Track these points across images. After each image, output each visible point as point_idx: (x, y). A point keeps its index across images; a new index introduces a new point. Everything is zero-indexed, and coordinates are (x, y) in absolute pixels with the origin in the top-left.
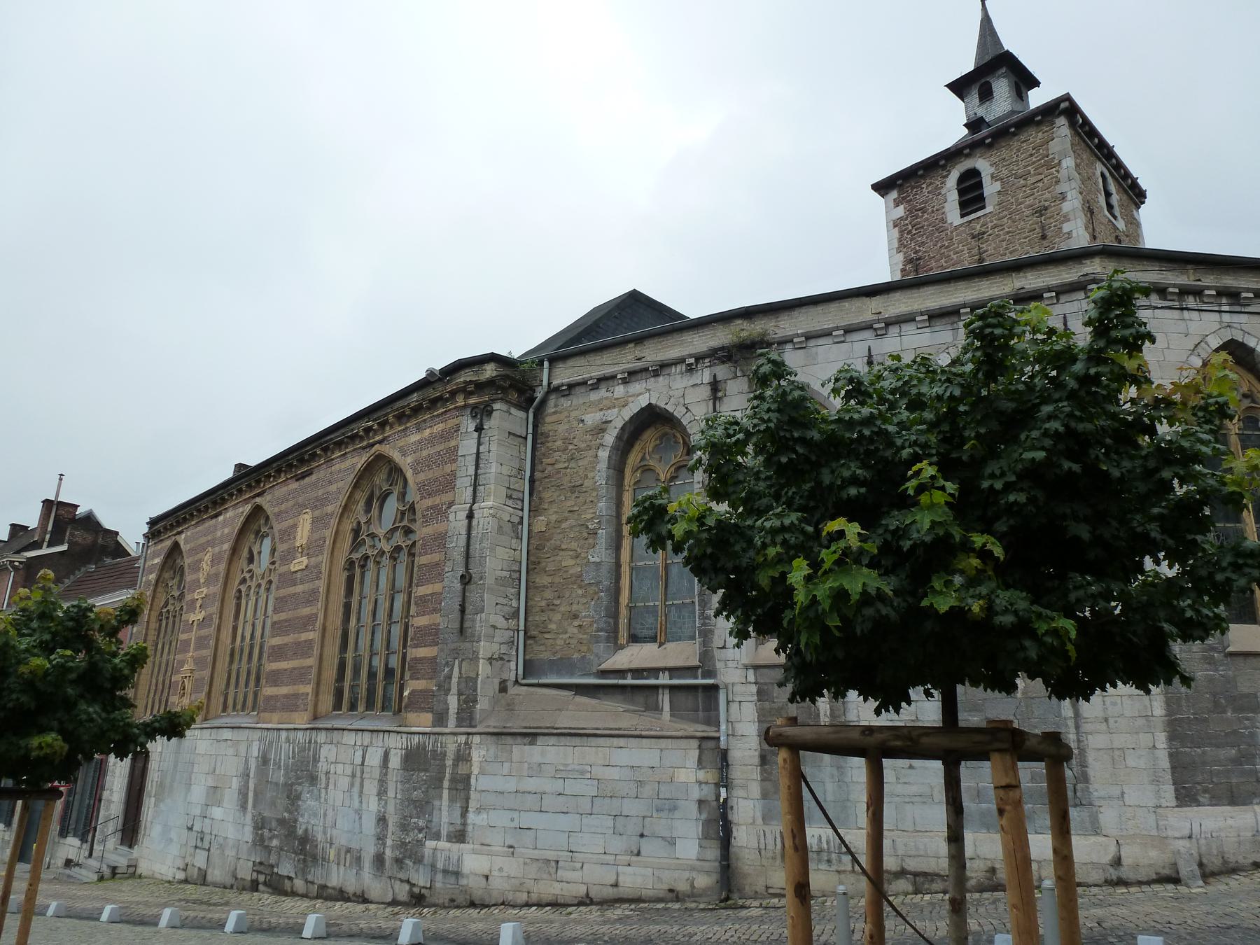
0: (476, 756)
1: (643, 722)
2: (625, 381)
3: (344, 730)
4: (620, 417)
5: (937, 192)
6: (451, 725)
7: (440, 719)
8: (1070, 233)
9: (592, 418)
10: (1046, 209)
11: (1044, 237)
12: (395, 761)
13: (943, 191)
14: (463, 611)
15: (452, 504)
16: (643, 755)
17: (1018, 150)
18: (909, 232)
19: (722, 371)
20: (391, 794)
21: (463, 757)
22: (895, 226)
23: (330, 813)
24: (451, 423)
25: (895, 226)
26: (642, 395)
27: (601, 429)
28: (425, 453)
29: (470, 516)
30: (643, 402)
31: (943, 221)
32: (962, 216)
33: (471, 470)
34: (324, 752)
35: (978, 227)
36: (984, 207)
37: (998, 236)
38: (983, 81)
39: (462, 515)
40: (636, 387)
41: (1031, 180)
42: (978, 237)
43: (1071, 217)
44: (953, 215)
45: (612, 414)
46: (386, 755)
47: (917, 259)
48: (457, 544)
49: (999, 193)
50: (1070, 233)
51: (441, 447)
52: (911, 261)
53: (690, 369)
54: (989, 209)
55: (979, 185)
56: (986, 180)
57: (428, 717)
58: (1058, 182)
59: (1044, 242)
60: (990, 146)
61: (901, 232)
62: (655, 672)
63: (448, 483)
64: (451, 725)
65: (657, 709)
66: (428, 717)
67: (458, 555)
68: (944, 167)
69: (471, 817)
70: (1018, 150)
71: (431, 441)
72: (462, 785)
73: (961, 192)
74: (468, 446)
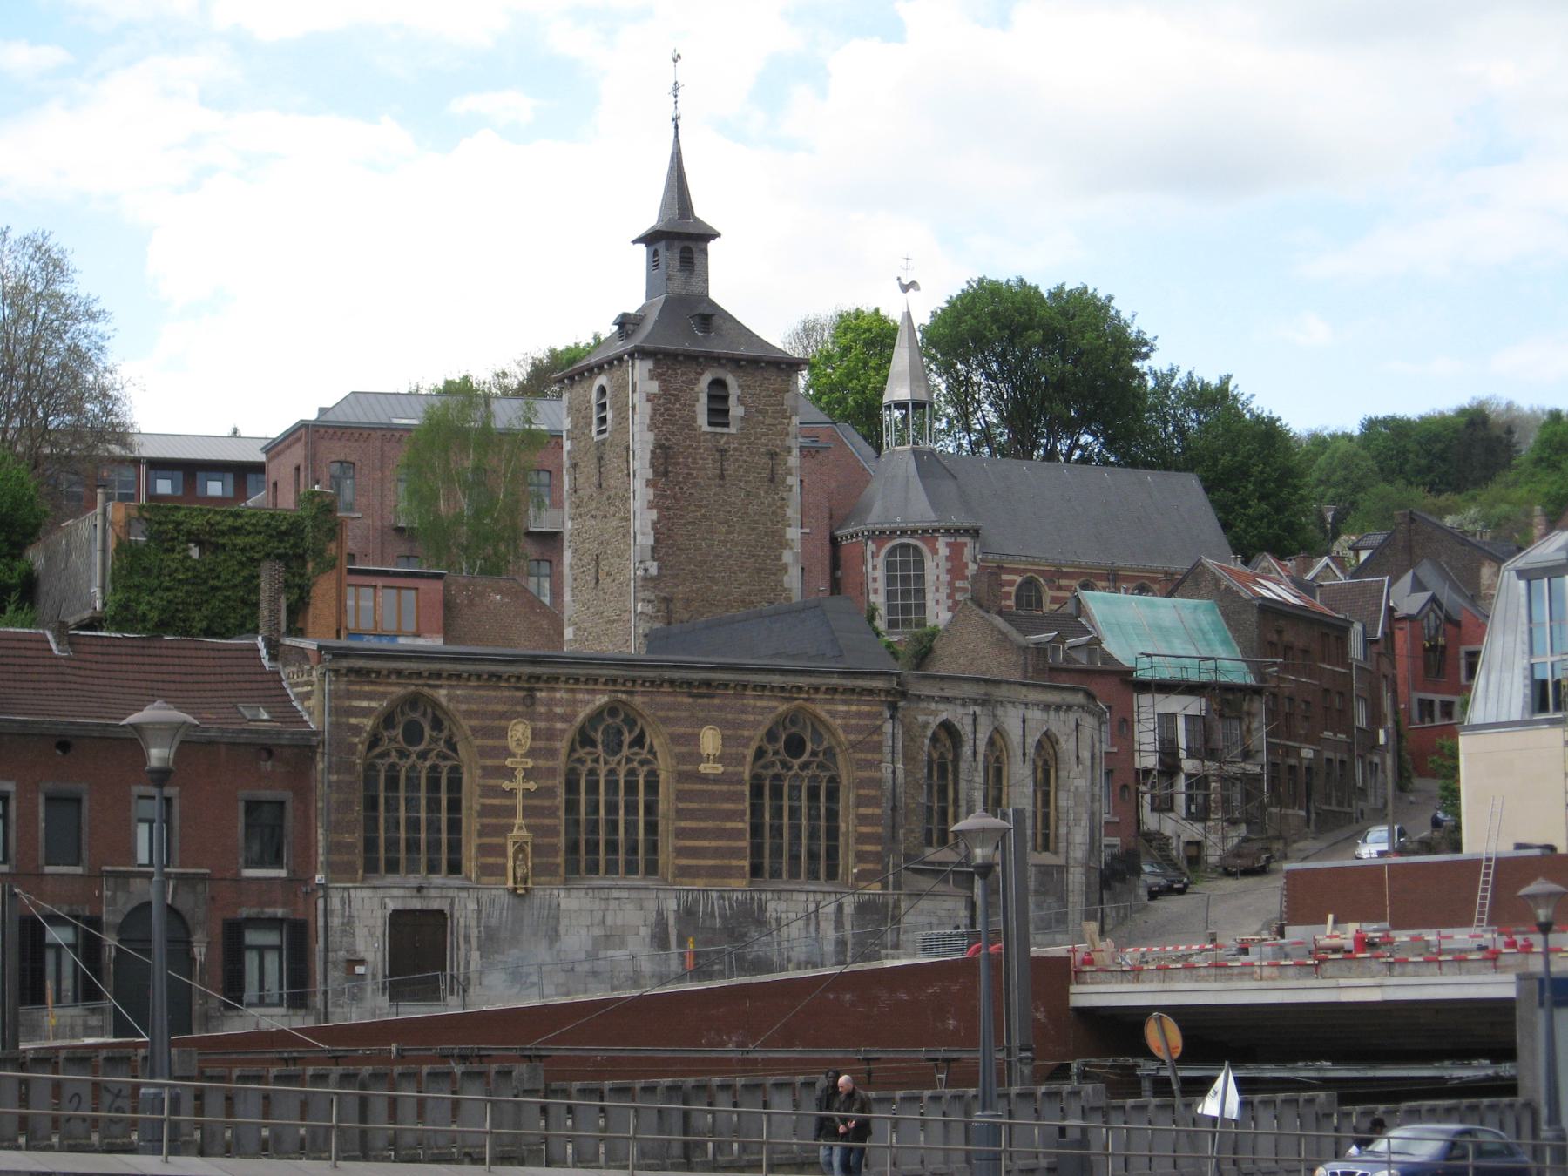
0: (903, 905)
1: (941, 888)
2: (937, 702)
3: (792, 891)
4: (934, 722)
5: (692, 383)
6: (890, 891)
7: (885, 886)
8: (791, 487)
9: (921, 718)
10: (776, 454)
11: (772, 480)
12: (849, 909)
13: (697, 389)
14: (893, 827)
15: (881, 762)
16: (949, 904)
17: (761, 385)
18: (662, 415)
19: (978, 709)
20: (848, 926)
21: (897, 905)
22: (648, 400)
23: (785, 944)
24: (875, 709)
25: (648, 400)
26: (946, 713)
27: (925, 725)
28: (853, 722)
29: (894, 772)
30: (944, 716)
31: (694, 419)
32: (710, 424)
33: (890, 743)
34: (771, 906)
35: (722, 442)
36: (727, 425)
37: (737, 460)
38: (686, 243)
39: (890, 770)
40: (941, 706)
41: (768, 421)
42: (723, 452)
43: (794, 471)
44: (702, 420)
45: (931, 719)
46: (840, 908)
47: (669, 448)
48: (888, 786)
49: (742, 418)
50: (791, 487)
51: (866, 722)
52: (661, 446)
53: (964, 705)
54: (733, 430)
55: (725, 398)
56: (732, 401)
57: (878, 885)
58: (787, 434)
59: (773, 486)
60: (740, 367)
61: (655, 410)
62: (946, 864)
63: (878, 747)
64: (890, 891)
65: (947, 882)
66: (879, 885)
67: (889, 795)
68: (699, 364)
69: (901, 936)
70: (761, 385)
71: (859, 715)
72: (896, 919)
73: (711, 398)
74: (888, 727)
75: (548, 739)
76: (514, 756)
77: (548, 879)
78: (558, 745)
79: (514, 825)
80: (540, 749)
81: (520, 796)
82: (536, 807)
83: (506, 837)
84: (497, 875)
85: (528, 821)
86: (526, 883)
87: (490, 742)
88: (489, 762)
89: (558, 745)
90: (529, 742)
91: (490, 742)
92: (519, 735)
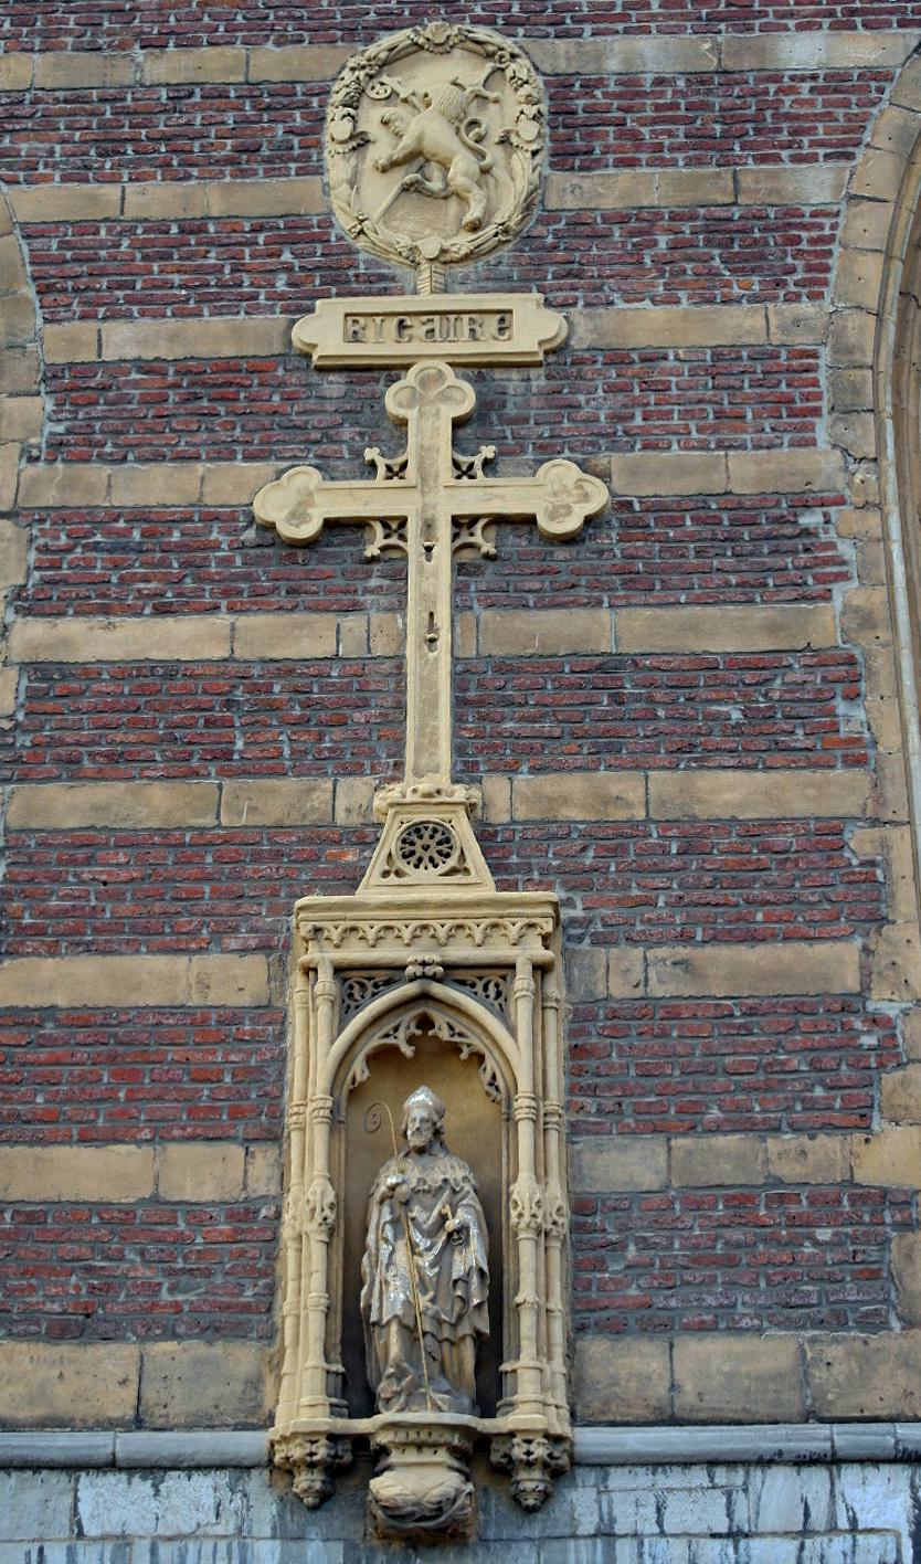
75: (702, 146)
76: (379, 283)
77: (773, 1352)
78: (814, 184)
79: (365, 837)
80: (640, 222)
81: (431, 578)
82: (607, 668)
83: (273, 947)
84: (155, 1324)
85: (507, 797)
86: (490, 1393)
87: (154, 198)
88: (125, 339)
89: (814, 184)
90: (519, 175)
91: (154, 198)
92: (432, 130)
